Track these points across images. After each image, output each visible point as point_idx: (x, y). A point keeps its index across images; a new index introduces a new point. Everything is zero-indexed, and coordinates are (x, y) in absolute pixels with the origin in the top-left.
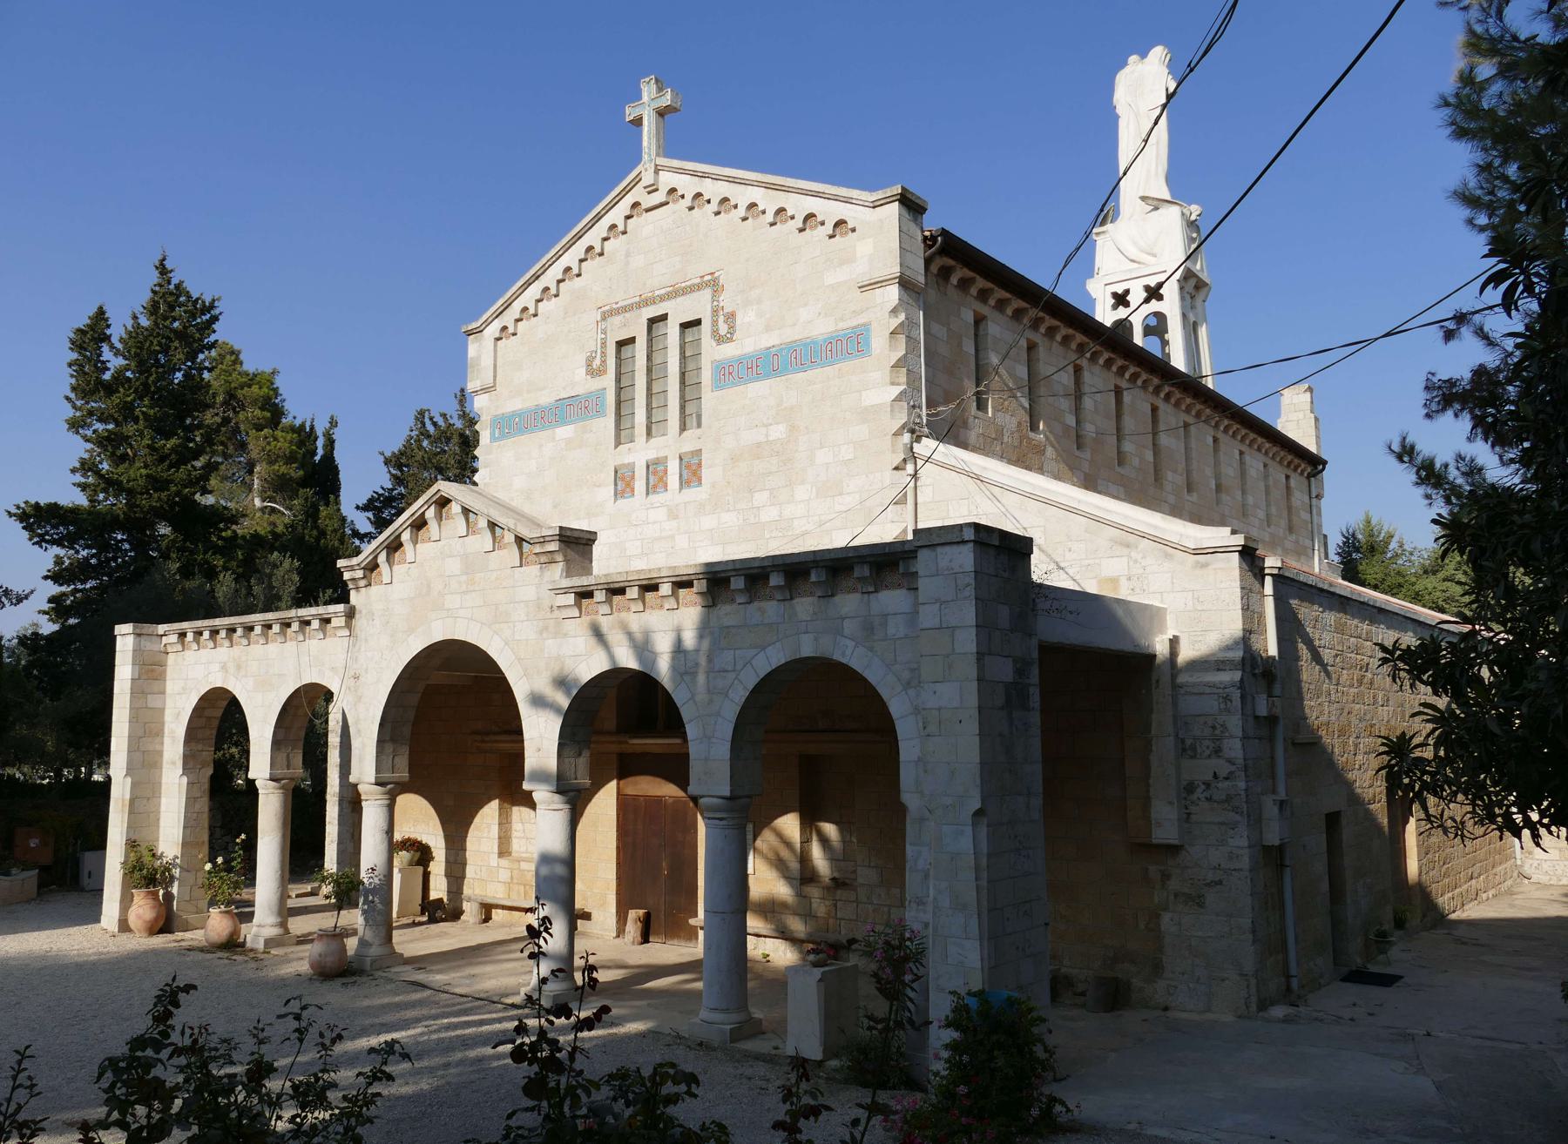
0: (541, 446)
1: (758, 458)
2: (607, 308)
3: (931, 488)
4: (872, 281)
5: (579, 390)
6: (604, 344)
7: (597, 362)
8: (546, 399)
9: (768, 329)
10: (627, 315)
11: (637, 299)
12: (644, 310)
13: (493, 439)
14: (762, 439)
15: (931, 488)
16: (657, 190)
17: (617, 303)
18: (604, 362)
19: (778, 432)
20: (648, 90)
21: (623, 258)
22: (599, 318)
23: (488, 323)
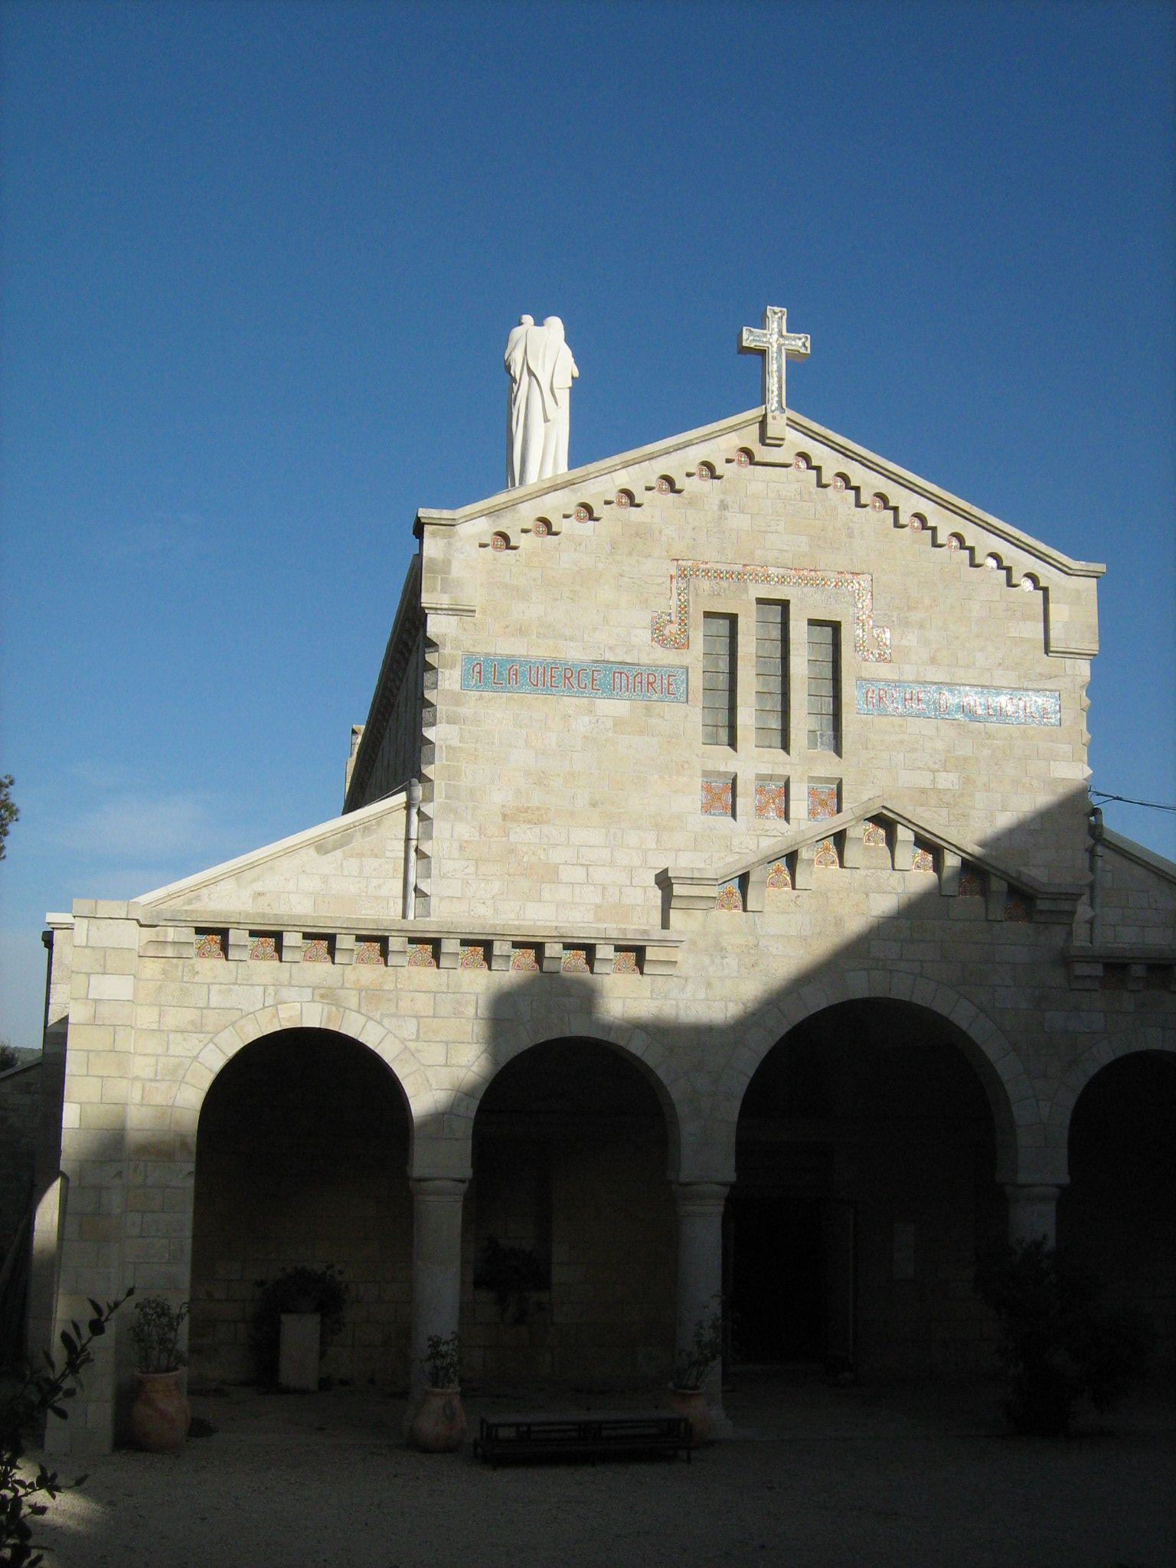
0: (566, 717)
1: (922, 805)
2: (690, 563)
3: (1110, 874)
4: (1068, 650)
5: (645, 659)
6: (683, 609)
7: (674, 628)
8: (575, 653)
9: (933, 661)
10: (724, 584)
11: (738, 568)
12: (751, 585)
13: (465, 686)
14: (928, 784)
15: (1110, 874)
16: (779, 446)
17: (706, 563)
18: (684, 631)
19: (947, 780)
20: (777, 317)
21: (716, 508)
22: (674, 572)
23: (471, 518)
